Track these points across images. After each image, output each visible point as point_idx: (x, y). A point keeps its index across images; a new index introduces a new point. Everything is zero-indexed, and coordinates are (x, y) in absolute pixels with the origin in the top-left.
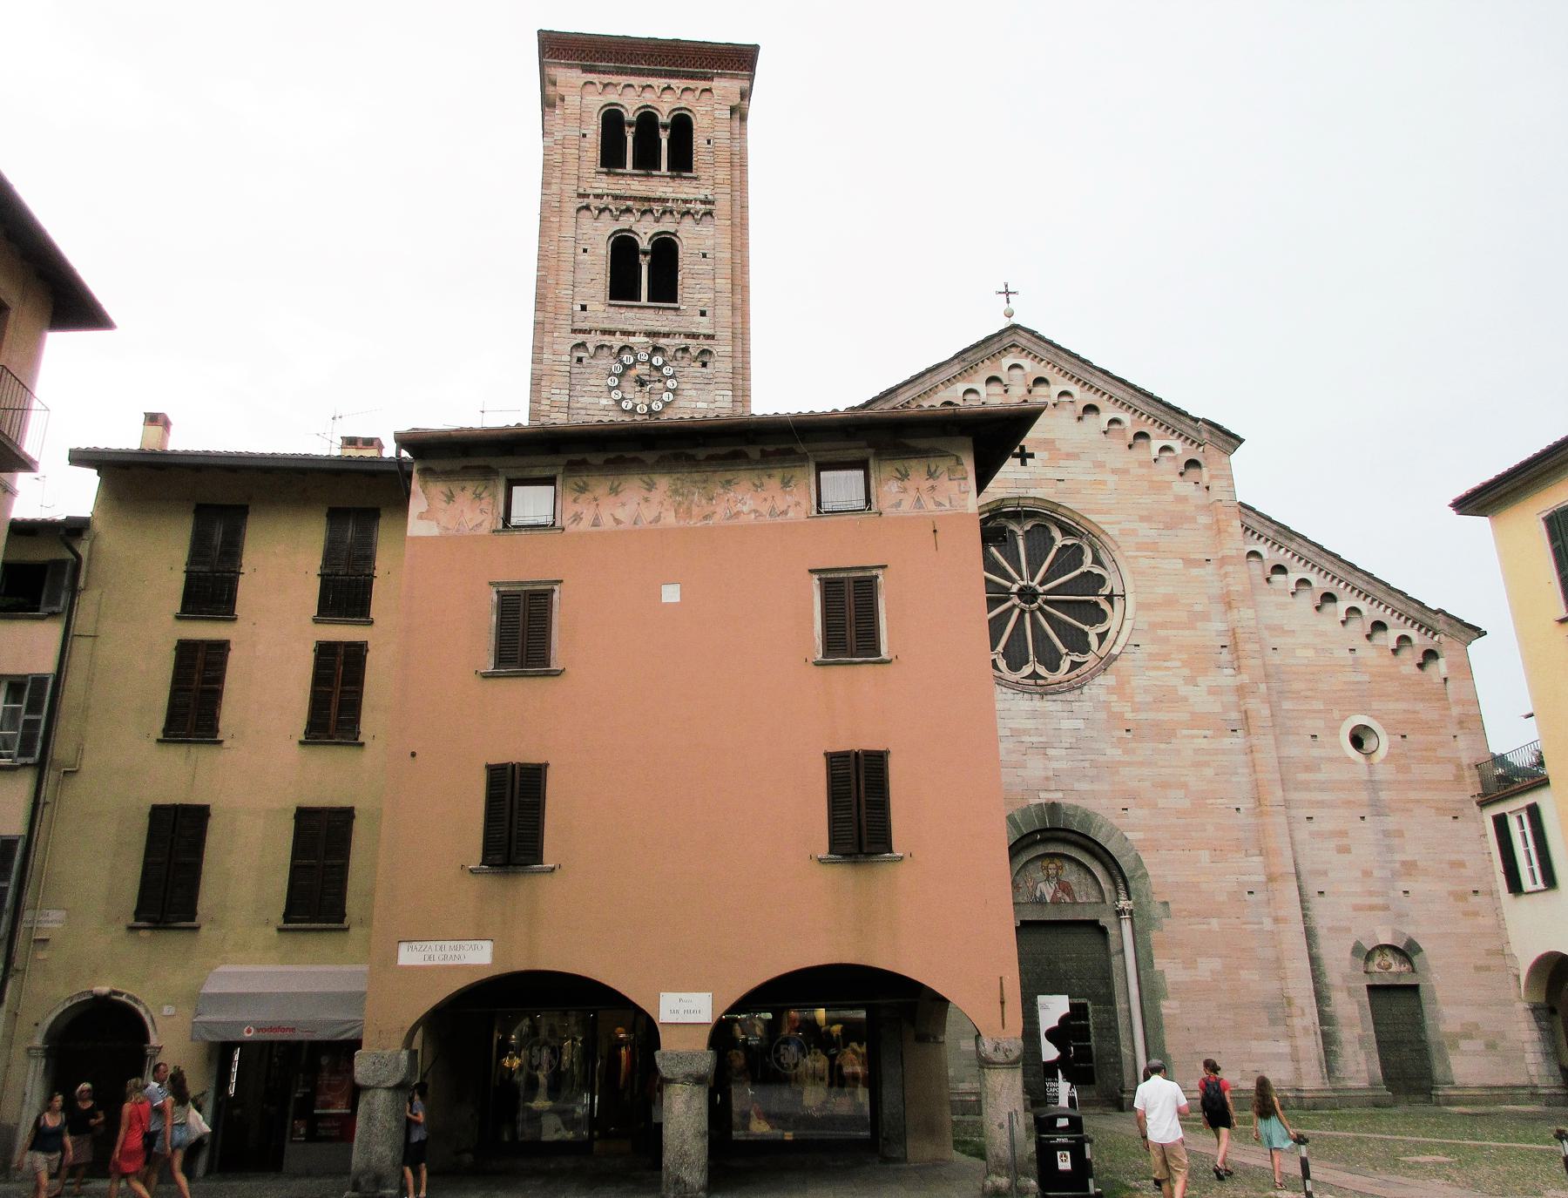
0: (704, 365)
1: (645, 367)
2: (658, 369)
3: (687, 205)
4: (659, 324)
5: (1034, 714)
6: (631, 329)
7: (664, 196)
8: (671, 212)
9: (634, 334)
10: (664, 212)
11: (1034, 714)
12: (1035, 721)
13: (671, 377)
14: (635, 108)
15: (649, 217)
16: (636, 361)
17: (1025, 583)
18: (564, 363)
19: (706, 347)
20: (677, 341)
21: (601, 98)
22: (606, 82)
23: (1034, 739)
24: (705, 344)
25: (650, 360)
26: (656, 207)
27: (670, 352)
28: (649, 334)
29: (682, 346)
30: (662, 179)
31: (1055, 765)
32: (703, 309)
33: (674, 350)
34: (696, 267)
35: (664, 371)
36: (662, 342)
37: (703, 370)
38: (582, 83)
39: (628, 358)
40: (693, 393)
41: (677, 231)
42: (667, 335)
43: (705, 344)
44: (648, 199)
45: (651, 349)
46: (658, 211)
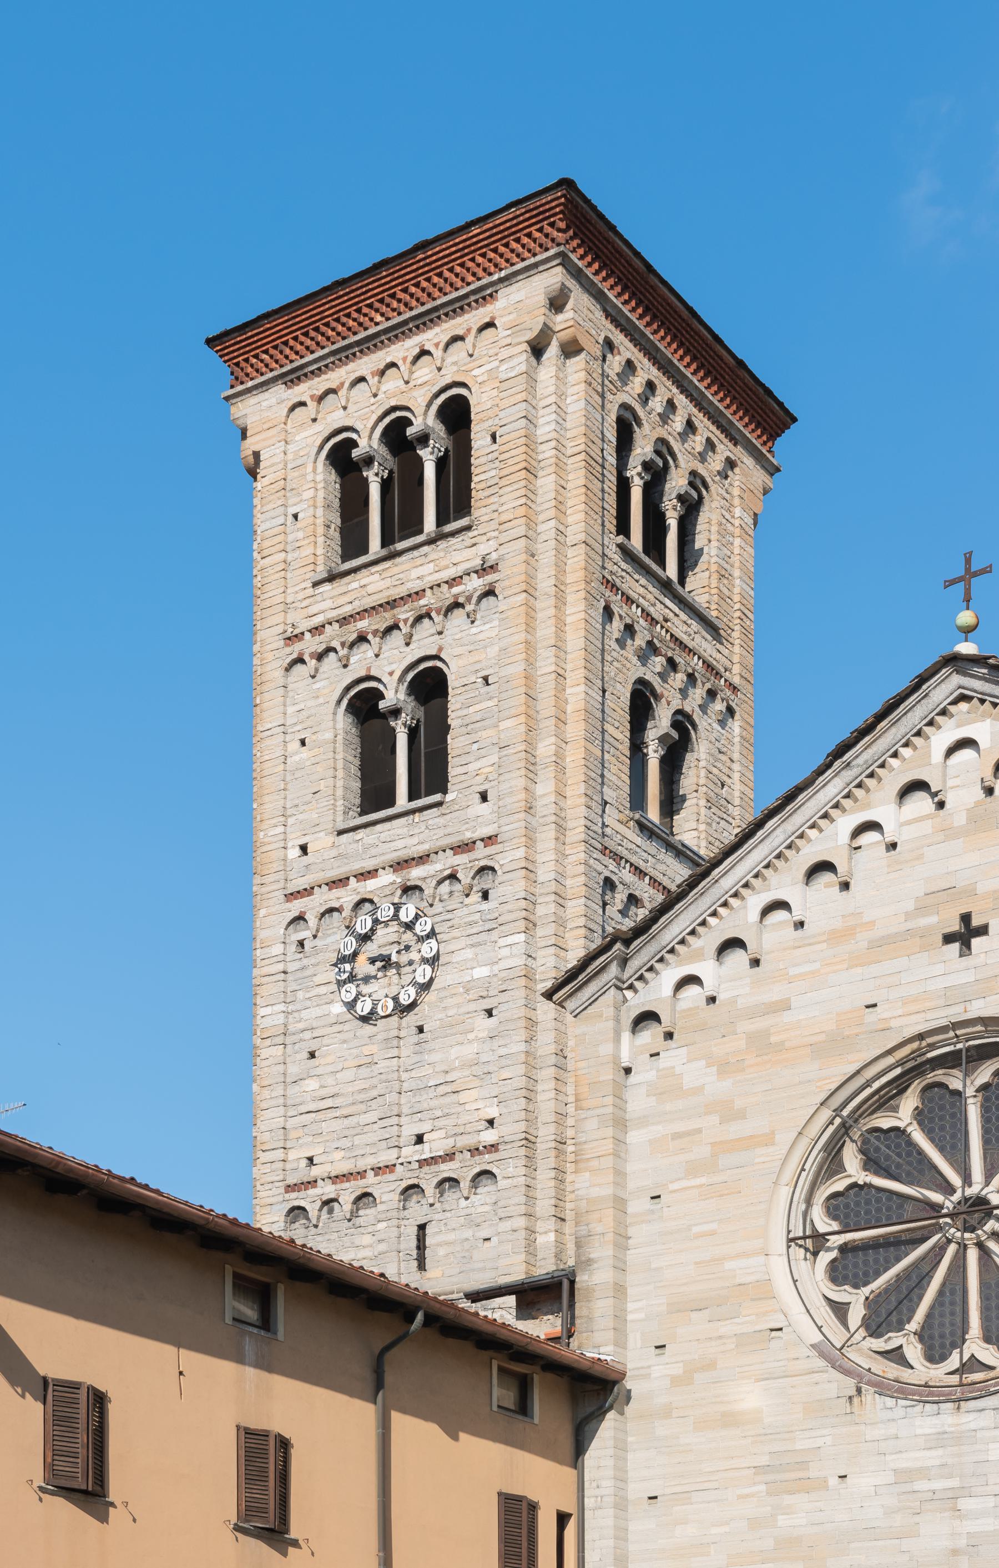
0: (485, 896)
1: (390, 929)
2: (409, 926)
3: (456, 590)
4: (415, 840)
5: (939, 1440)
6: (369, 865)
7: (415, 586)
8: (428, 615)
9: (372, 873)
10: (419, 619)
11: (939, 1440)
12: (940, 1452)
13: (428, 936)
14: (370, 424)
15: (396, 638)
16: (376, 922)
17: (971, 1191)
18: (275, 959)
19: (482, 863)
20: (438, 866)
21: (318, 427)
22: (319, 393)
23: (938, 1485)
24: (481, 854)
25: (396, 917)
26: (405, 614)
27: (428, 891)
28: (400, 865)
29: (448, 872)
30: (416, 553)
31: (971, 1526)
32: (481, 789)
33: (434, 882)
34: (471, 710)
35: (418, 928)
36: (415, 874)
37: (485, 906)
38: (286, 410)
39: (363, 924)
40: (469, 953)
41: (441, 649)
42: (423, 859)
43: (481, 854)
44: (392, 604)
45: (399, 892)
46: (406, 621)
